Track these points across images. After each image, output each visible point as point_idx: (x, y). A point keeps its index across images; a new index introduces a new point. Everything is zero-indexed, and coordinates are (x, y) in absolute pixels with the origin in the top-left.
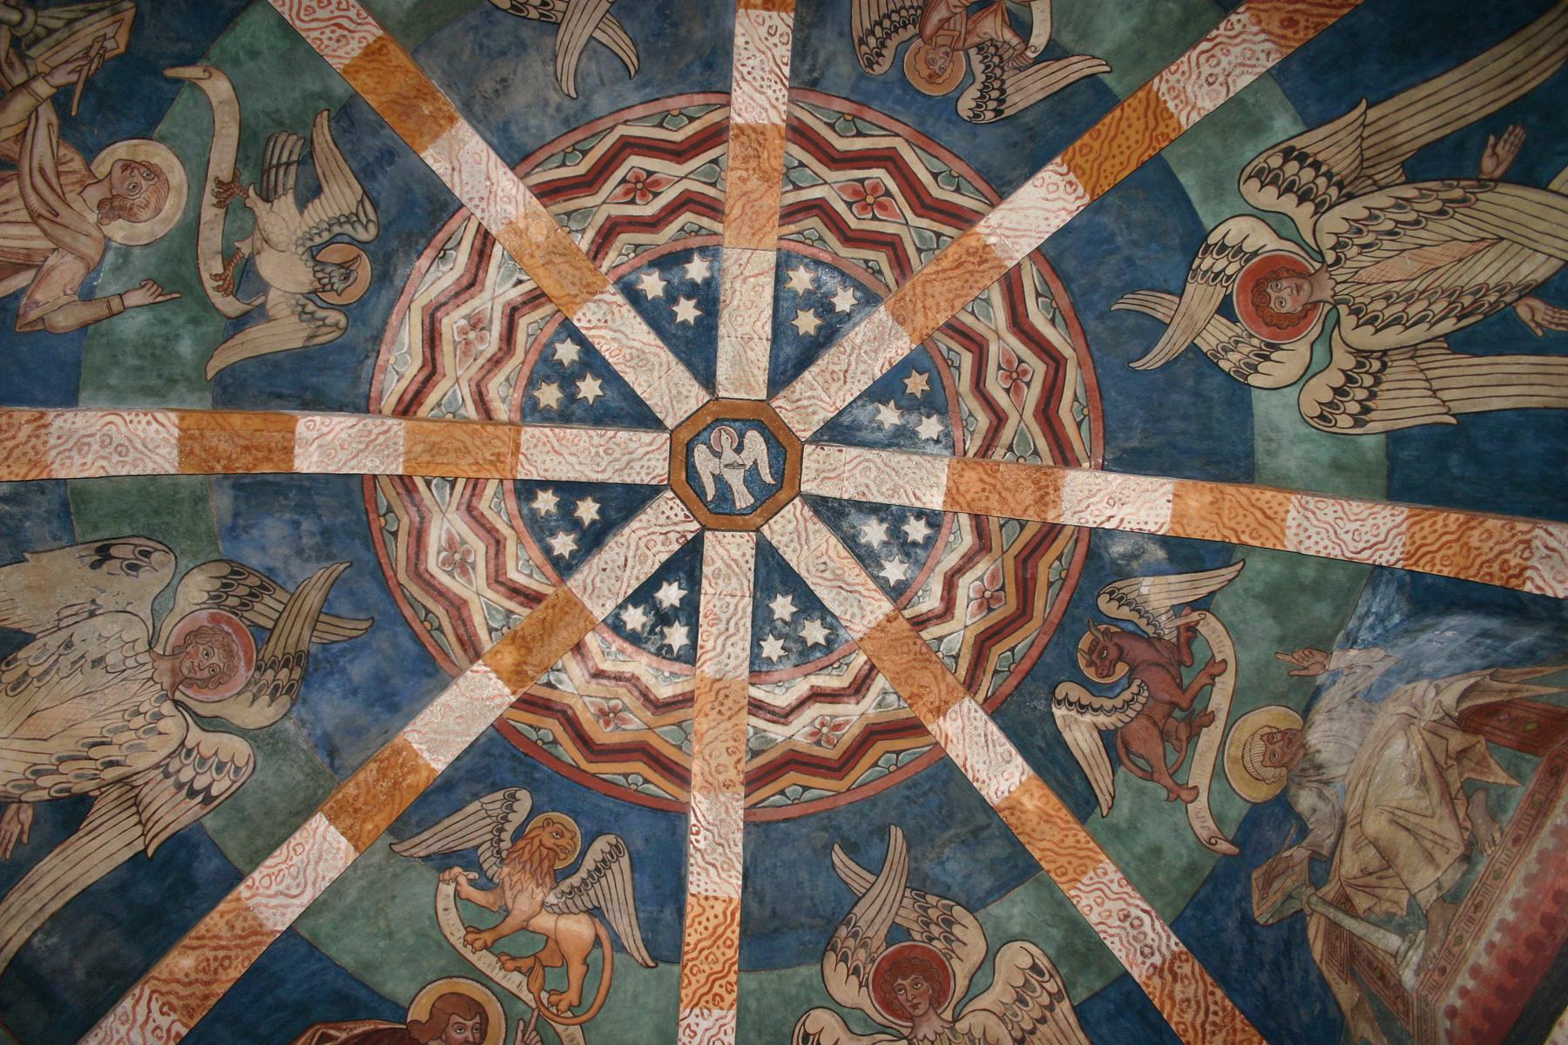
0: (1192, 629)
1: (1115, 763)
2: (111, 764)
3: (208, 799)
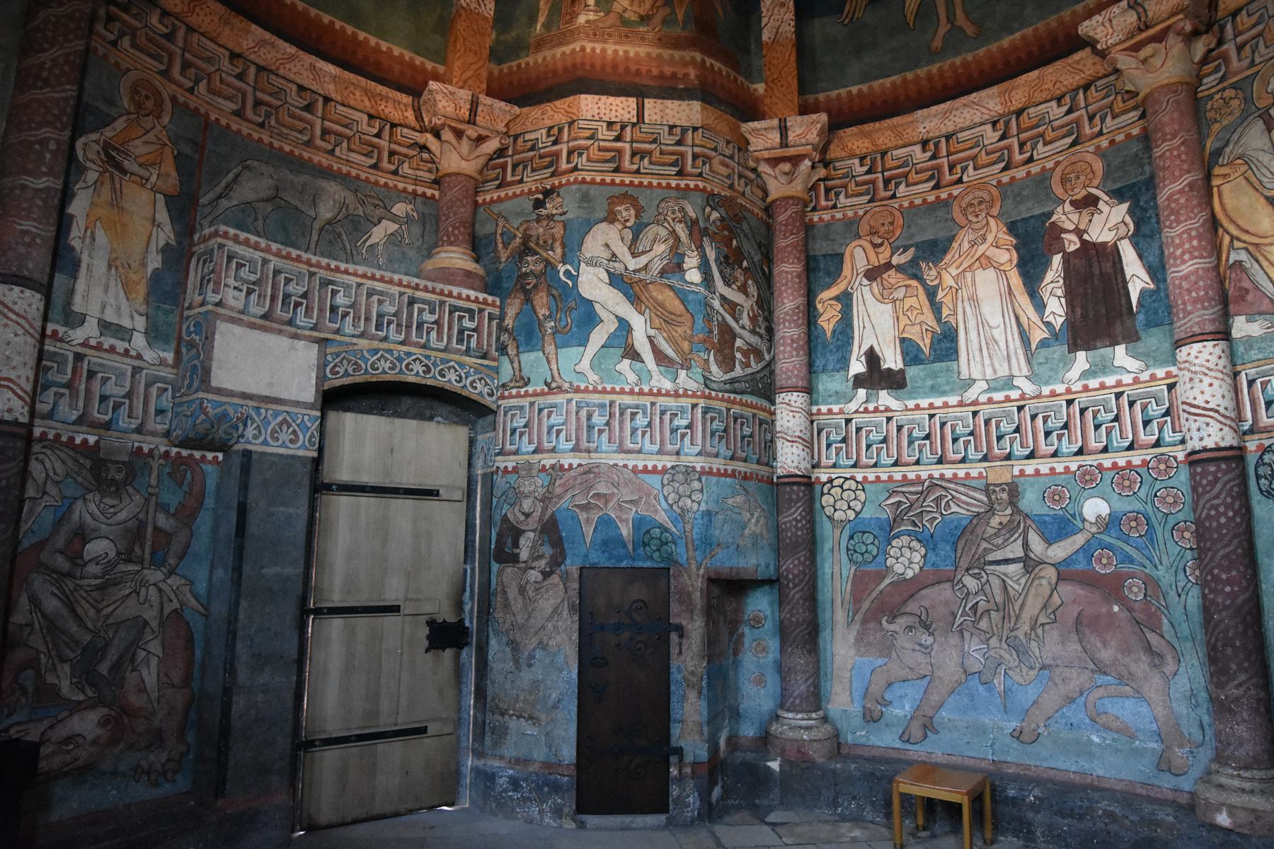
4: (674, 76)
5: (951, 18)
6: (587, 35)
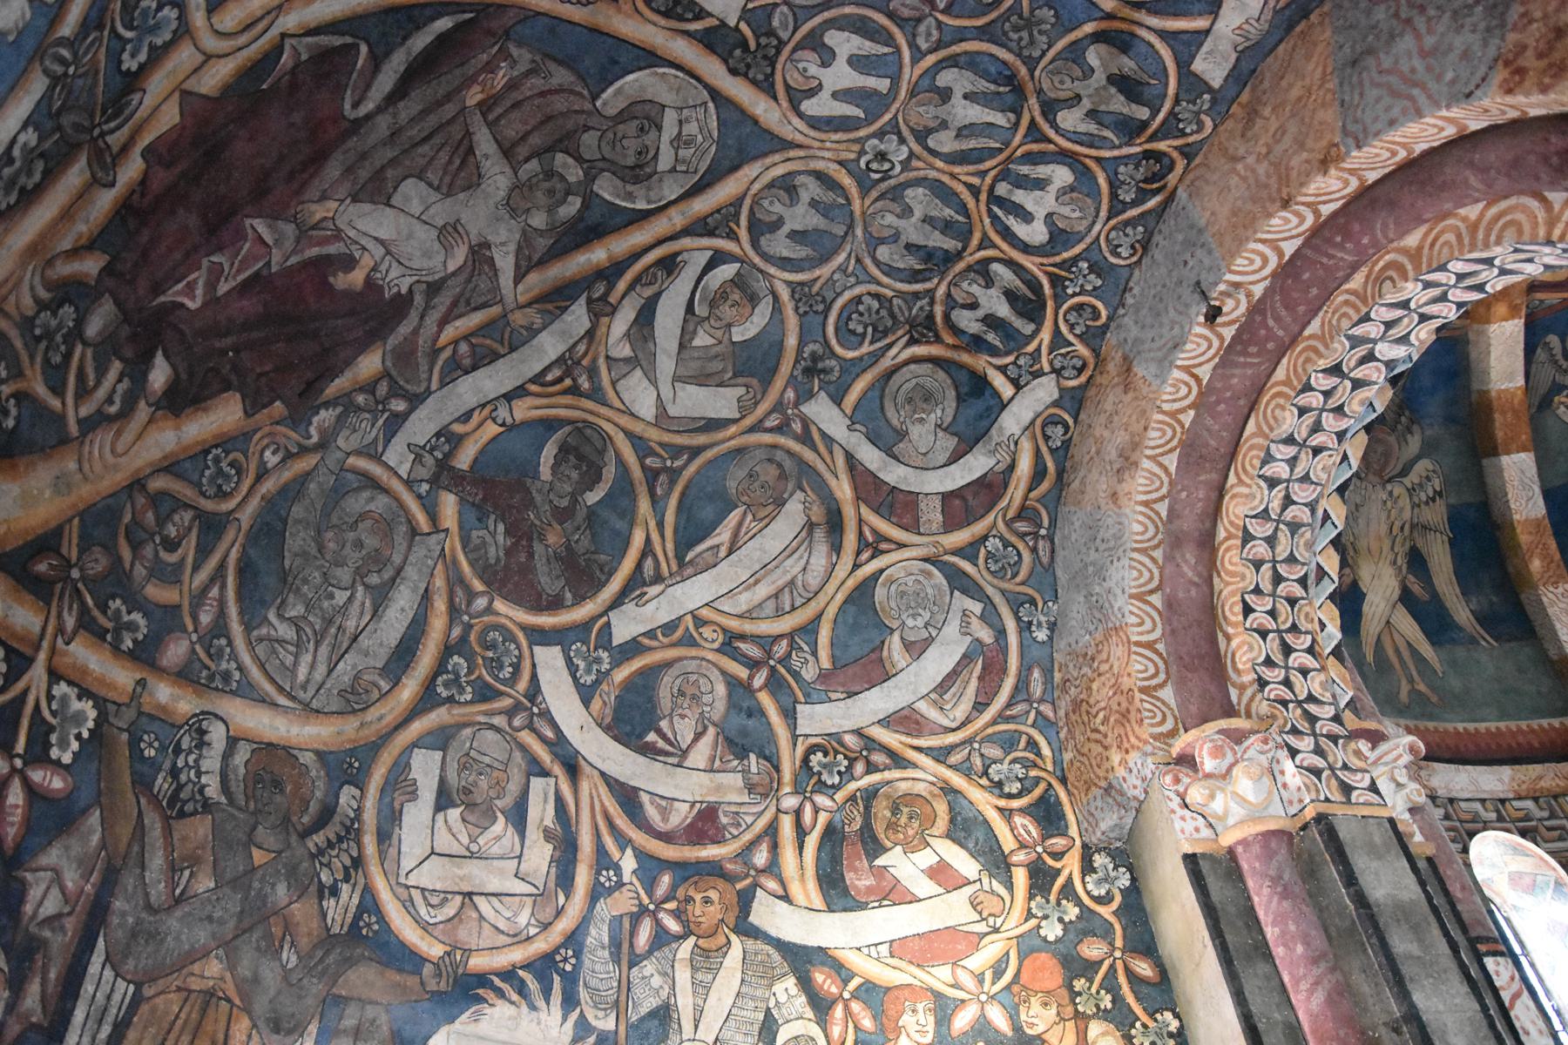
2: (1402, 528)
3: (1440, 494)
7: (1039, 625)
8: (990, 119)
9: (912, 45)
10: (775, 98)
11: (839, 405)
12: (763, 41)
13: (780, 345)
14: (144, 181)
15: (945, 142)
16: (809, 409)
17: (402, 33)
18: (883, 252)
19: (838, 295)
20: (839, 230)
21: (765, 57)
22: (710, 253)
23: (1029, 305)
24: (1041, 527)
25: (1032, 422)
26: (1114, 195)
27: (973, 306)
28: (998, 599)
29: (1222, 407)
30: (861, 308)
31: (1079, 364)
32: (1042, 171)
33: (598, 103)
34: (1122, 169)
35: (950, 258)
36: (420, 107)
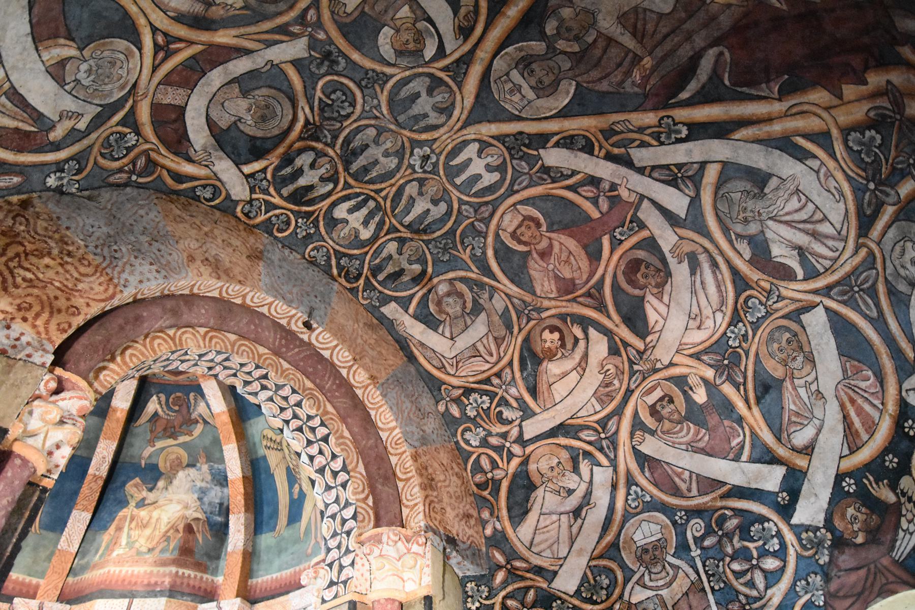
0: (197, 422)
1: (149, 421)
4: (156, 584)
5: (316, 538)
6: (114, 563)
7: (61, 178)
8: (411, 214)
9: (467, 203)
10: (492, 137)
11: (291, 62)
12: (521, 153)
13: (358, 49)
14: (866, 68)
15: (411, 189)
16: (303, 42)
17: (706, 89)
18: (372, 132)
19: (364, 97)
20: (401, 118)
21: (514, 148)
22: (448, 52)
23: (300, 196)
24: (139, 176)
25: (220, 180)
26: (345, 255)
27: (312, 166)
28: (86, 142)
29: (253, 327)
30: (346, 104)
31: (252, 215)
32: (372, 226)
33: (574, 83)
34: (358, 262)
35: (347, 164)
36: (678, 53)
